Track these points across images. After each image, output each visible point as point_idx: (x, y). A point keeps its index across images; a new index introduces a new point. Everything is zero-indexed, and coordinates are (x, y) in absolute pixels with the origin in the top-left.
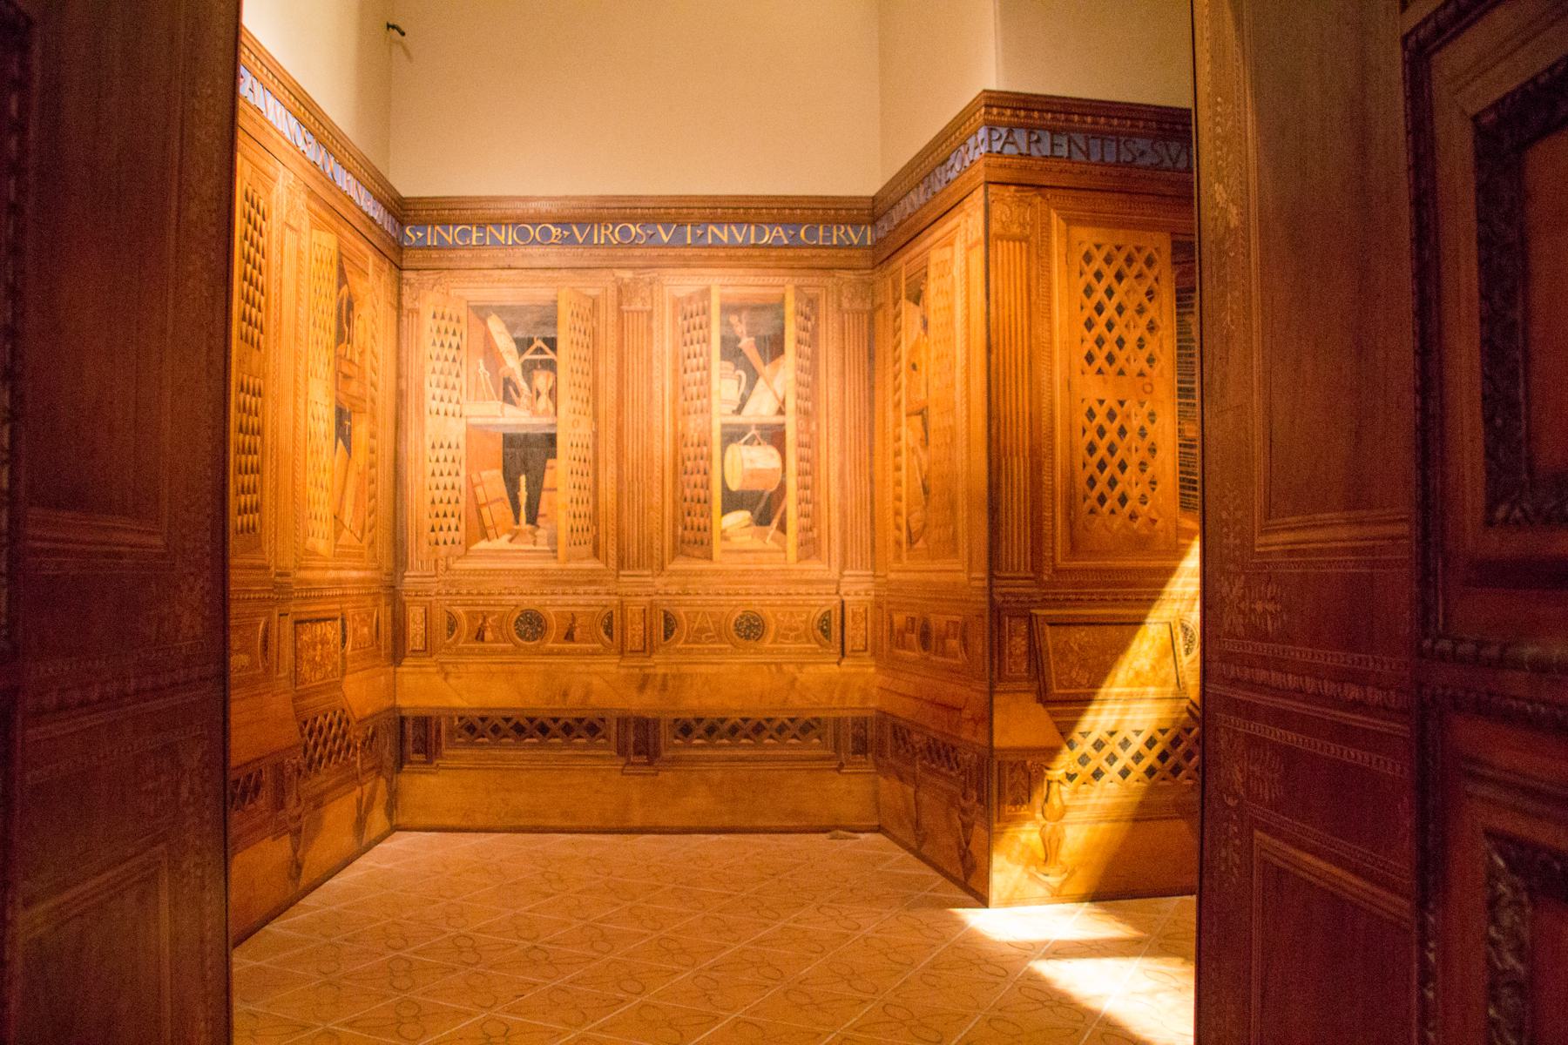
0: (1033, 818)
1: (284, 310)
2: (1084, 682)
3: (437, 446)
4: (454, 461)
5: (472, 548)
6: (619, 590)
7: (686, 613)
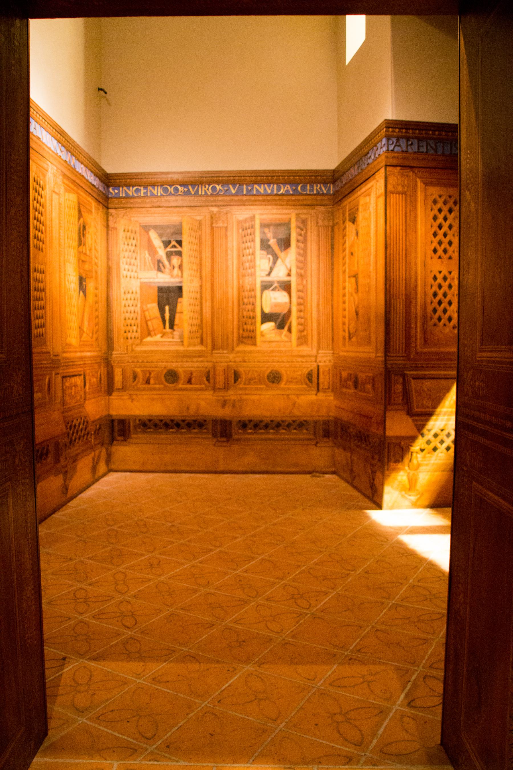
0: (404, 469)
1: (54, 232)
2: (430, 406)
3: (127, 292)
4: (134, 299)
5: (145, 340)
6: (213, 360)
7: (244, 371)
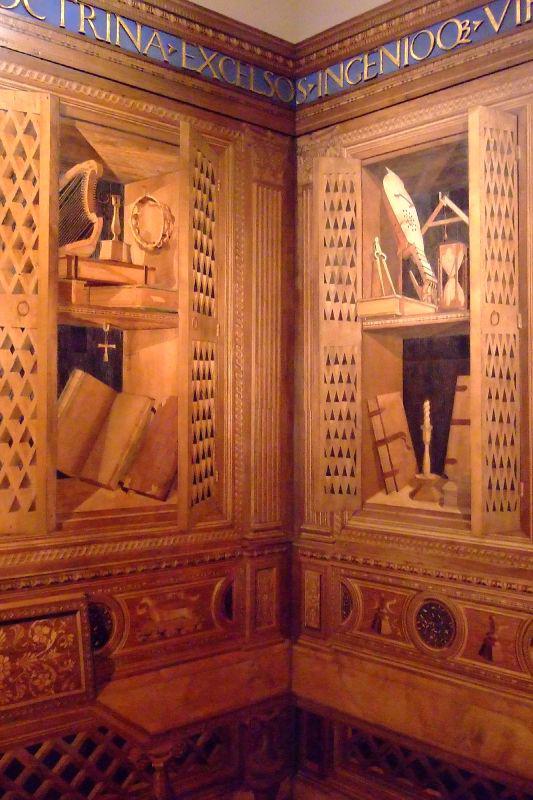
4: (349, 381)
5: (371, 501)
